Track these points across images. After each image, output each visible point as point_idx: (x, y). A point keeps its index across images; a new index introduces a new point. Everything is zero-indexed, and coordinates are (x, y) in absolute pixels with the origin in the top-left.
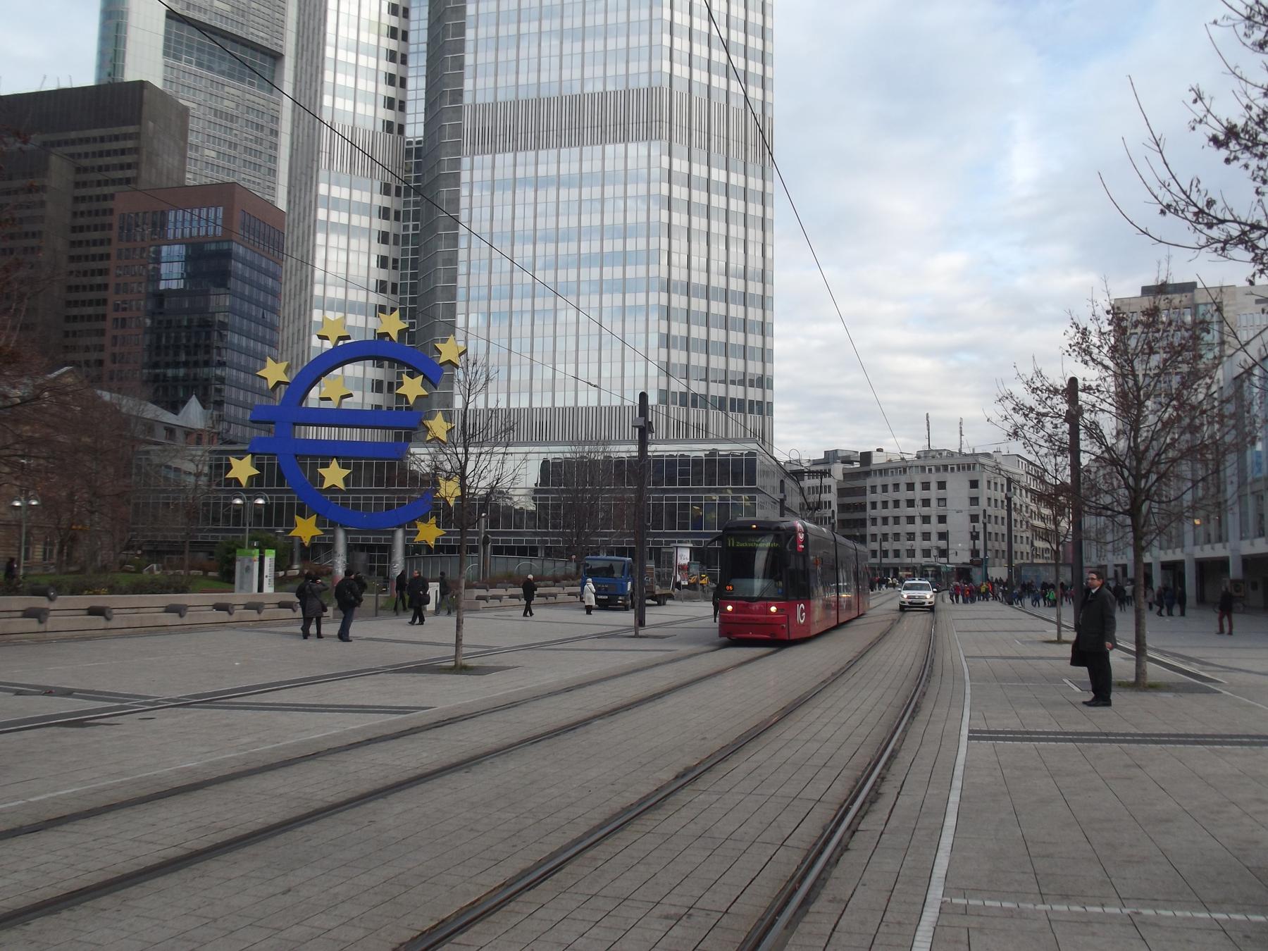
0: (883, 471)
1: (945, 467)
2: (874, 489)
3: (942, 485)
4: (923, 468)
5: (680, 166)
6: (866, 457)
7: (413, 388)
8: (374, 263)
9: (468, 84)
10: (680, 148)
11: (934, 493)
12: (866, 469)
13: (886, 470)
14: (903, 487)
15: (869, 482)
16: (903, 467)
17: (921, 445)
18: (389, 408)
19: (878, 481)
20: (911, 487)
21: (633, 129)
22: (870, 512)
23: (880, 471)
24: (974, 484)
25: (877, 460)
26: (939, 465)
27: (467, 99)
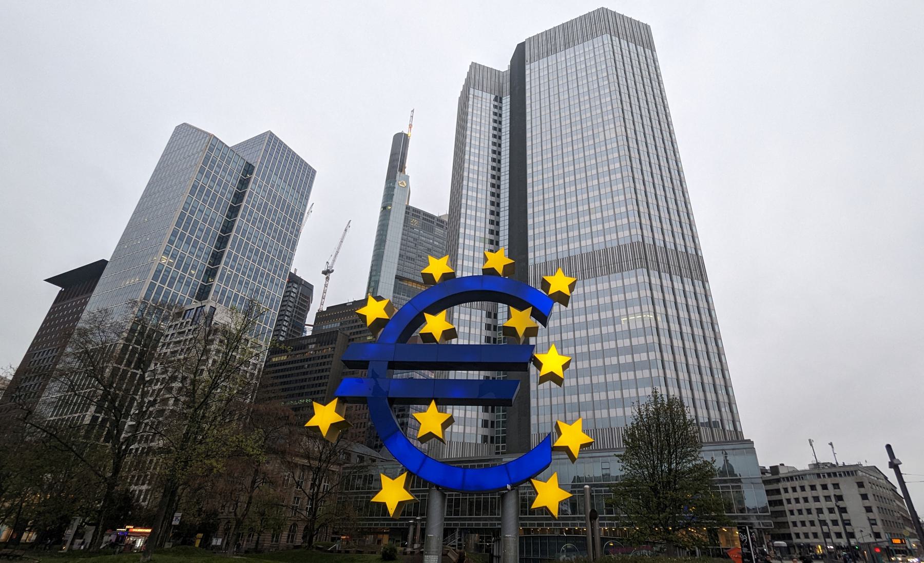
0: (790, 478)
1: (835, 474)
2: (786, 490)
3: (836, 486)
4: (819, 475)
5: (655, 280)
6: (775, 470)
7: (520, 320)
8: (484, 328)
9: (531, 255)
10: (654, 274)
11: (831, 491)
12: (776, 477)
13: (792, 478)
14: (808, 488)
15: (781, 486)
16: (801, 476)
17: (812, 460)
18: (494, 378)
19: (789, 485)
20: (813, 488)
21: (625, 264)
22: (787, 507)
23: (787, 478)
24: (861, 485)
25: (782, 471)
26: (828, 474)
27: (531, 262)
